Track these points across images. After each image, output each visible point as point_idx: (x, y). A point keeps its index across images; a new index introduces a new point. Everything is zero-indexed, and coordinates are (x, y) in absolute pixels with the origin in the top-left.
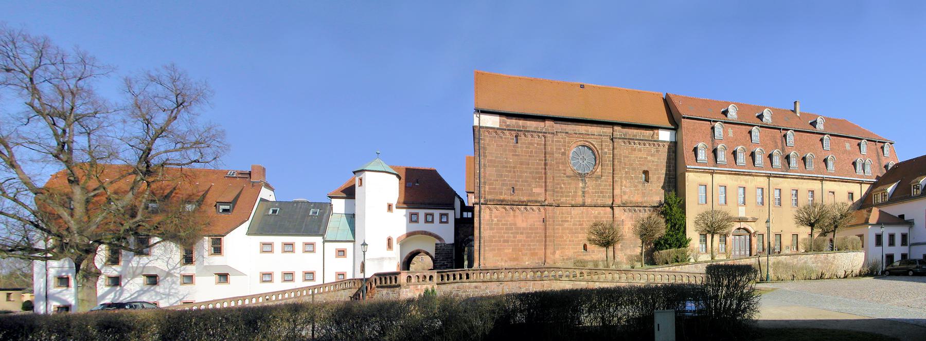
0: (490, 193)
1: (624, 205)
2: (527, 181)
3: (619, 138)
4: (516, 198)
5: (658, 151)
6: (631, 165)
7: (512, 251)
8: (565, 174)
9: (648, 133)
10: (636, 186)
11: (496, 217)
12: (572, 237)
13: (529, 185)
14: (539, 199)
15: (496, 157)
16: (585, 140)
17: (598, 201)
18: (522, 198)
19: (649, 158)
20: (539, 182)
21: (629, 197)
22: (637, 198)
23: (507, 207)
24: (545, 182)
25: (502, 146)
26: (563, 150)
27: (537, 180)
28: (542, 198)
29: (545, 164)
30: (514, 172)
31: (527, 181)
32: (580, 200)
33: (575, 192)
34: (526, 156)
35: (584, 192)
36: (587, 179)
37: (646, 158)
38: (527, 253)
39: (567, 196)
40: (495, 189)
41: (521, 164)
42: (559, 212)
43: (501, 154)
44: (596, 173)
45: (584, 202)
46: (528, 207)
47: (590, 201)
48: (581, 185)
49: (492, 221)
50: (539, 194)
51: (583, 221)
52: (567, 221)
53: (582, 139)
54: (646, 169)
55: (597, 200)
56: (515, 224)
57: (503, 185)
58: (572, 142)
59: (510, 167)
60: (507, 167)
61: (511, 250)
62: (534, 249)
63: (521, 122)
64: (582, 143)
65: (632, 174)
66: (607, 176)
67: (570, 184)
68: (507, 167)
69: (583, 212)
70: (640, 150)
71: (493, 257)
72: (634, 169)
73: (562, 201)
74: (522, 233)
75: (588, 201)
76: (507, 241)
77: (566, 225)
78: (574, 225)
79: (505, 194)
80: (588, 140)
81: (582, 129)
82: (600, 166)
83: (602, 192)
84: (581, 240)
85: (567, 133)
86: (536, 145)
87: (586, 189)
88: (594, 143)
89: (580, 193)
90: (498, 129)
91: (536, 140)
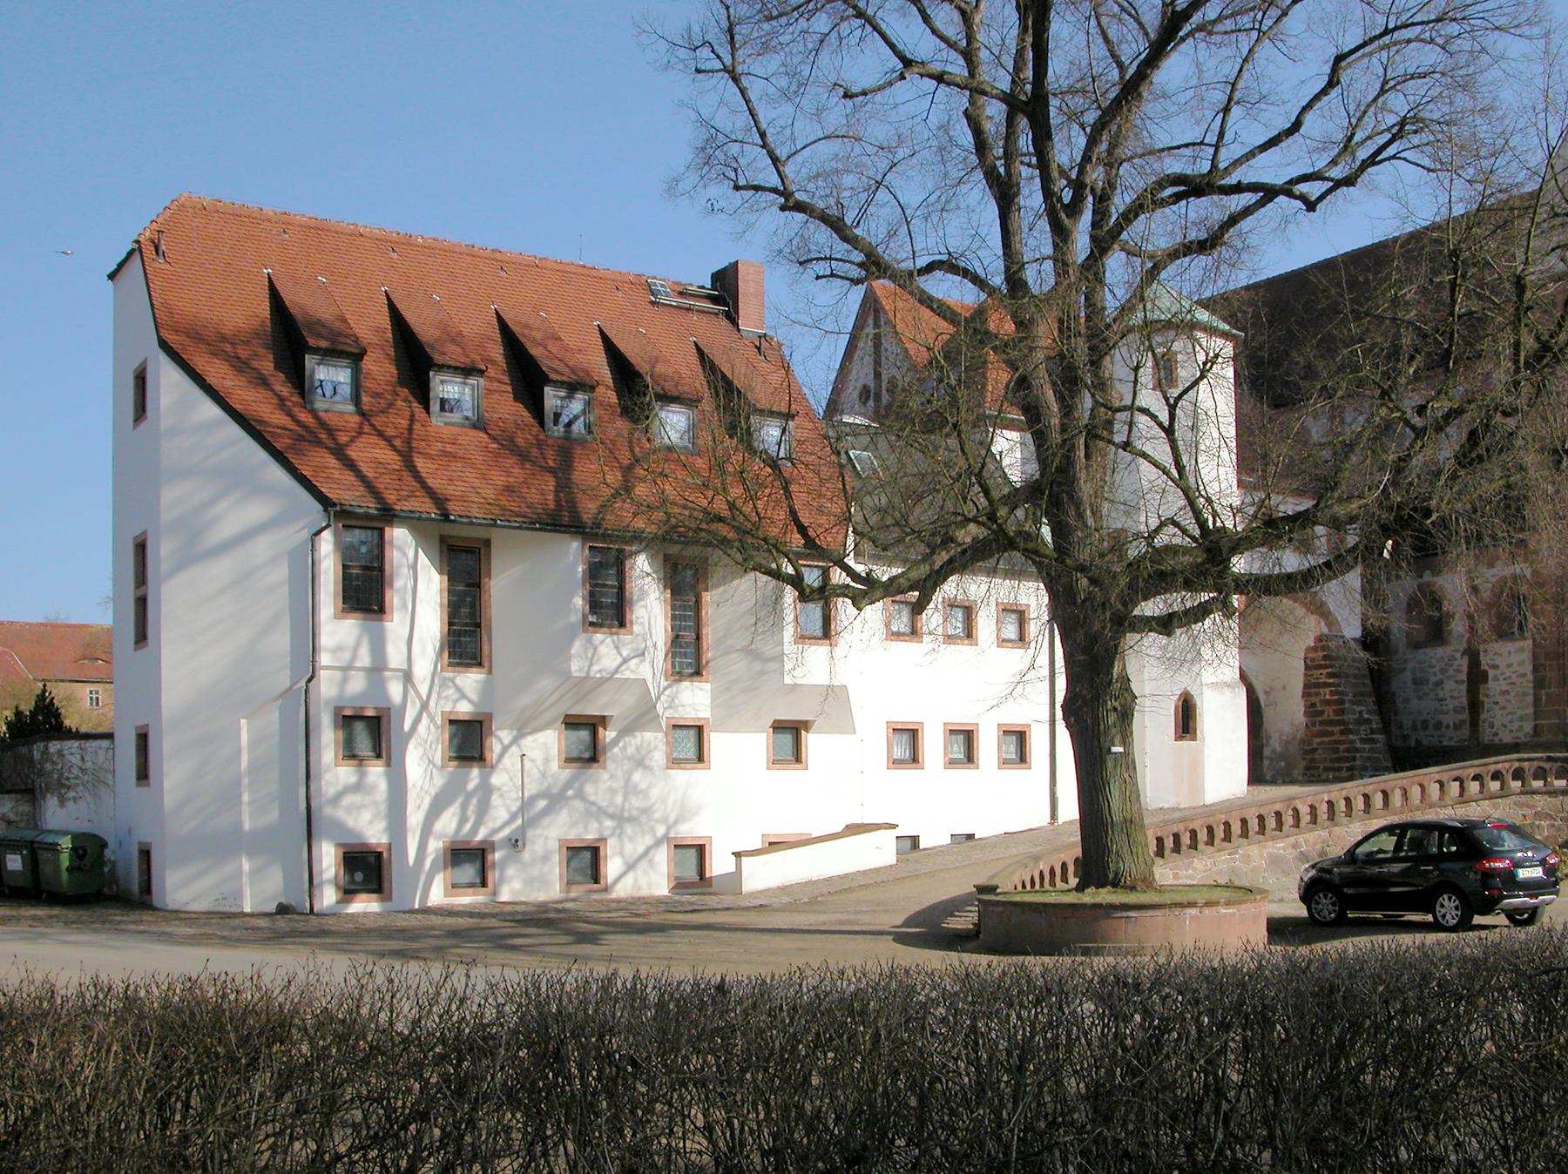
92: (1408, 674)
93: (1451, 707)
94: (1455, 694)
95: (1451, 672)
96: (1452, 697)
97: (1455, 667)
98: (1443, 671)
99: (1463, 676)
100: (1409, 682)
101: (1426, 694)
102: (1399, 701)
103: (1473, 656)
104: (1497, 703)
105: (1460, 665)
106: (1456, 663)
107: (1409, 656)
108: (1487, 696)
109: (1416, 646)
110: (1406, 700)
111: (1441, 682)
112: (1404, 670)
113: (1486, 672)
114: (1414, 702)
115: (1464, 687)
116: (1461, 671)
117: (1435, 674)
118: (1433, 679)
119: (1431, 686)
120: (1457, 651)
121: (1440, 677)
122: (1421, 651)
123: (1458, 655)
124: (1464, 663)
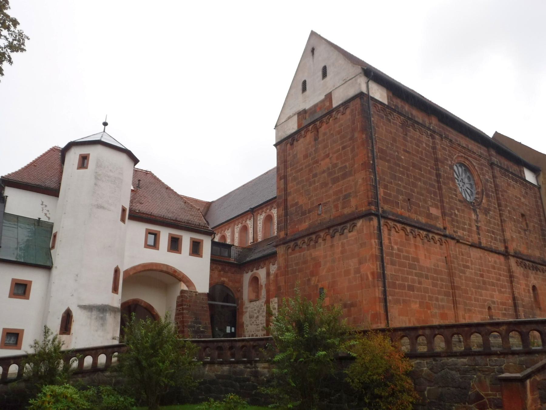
0: (386, 201)
1: (517, 255)
2: (422, 195)
3: (498, 166)
4: (414, 217)
5: (526, 193)
6: (511, 203)
7: (420, 306)
8: (456, 195)
9: (514, 168)
10: (520, 233)
11: (396, 244)
12: (476, 293)
13: (425, 201)
14: (438, 225)
15: (387, 147)
16: (466, 156)
17: (492, 244)
18: (420, 218)
19: (523, 200)
20: (434, 199)
21: (517, 245)
22: (523, 249)
23: (408, 229)
24: (442, 201)
25: (391, 133)
26: (450, 163)
27: (432, 196)
28: (440, 225)
29: (438, 175)
30: (408, 176)
31: (422, 195)
32: (474, 238)
33: (470, 225)
34: (417, 157)
35: (478, 228)
36: (478, 210)
37: (520, 199)
38: (436, 313)
39: (464, 229)
40: (390, 195)
41: (414, 166)
42: (459, 251)
43: (392, 145)
44: (482, 205)
45: (480, 243)
46: (431, 235)
47: (484, 242)
48: (474, 217)
49: (392, 249)
50: (437, 218)
51: (483, 271)
52: (468, 267)
53: (463, 155)
54: (523, 212)
55: (491, 242)
56: (417, 260)
57: (399, 192)
58: (455, 155)
59: (403, 167)
60: (399, 166)
61: (418, 305)
62: (443, 307)
63: (407, 108)
64: (462, 160)
65: (514, 216)
66: (494, 212)
67: (463, 211)
68: (399, 166)
69: (481, 256)
70: (514, 187)
71: (399, 315)
72: (514, 210)
73: (459, 234)
74: (427, 277)
75: (484, 243)
76: (411, 288)
77: (468, 271)
78: (476, 274)
79: (402, 208)
80: (469, 158)
81: (464, 141)
82: (484, 196)
83: (493, 233)
84: (485, 301)
85: (451, 141)
86: (424, 145)
87: (479, 225)
88: (475, 164)
89: (474, 228)
90: (388, 107)
91: (424, 138)
93: (261, 328)
94: (262, 322)
95: (261, 312)
96: (261, 324)
98: (259, 312)
99: (264, 314)
101: (253, 322)
102: (245, 326)
103: (268, 302)
105: (263, 309)
106: (262, 308)
107: (248, 306)
109: (251, 301)
110: (247, 326)
111: (257, 317)
112: (246, 312)
114: (250, 326)
115: (265, 319)
117: (256, 314)
118: (255, 315)
119: (254, 319)
120: (263, 302)
121: (258, 314)
123: (263, 304)
124: (265, 307)
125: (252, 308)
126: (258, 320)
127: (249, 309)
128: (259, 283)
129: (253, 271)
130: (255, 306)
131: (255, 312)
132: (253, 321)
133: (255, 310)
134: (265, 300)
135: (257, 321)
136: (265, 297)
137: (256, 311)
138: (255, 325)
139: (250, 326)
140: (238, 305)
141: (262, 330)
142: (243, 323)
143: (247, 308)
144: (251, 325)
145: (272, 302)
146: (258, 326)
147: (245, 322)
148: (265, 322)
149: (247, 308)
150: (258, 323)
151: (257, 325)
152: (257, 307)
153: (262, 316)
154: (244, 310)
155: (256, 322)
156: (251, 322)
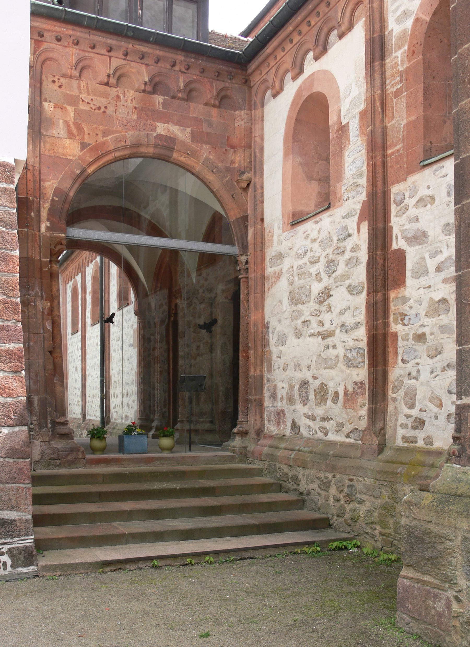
92: (283, 284)
93: (340, 351)
94: (349, 319)
95: (341, 268)
97: (347, 255)
100: (286, 301)
101: (306, 323)
104: (420, 338)
105: (354, 249)
106: (349, 244)
107: (282, 249)
108: (402, 317)
110: (282, 341)
112: (278, 276)
113: (401, 254)
114: (292, 340)
116: (358, 263)
117: (318, 277)
118: (317, 288)
119: (312, 306)
121: (326, 281)
122: (301, 228)
123: (352, 223)
125: (299, 256)
126: (329, 309)
127: (286, 264)
128: (333, 119)
129: (301, 71)
130: (314, 240)
131: (314, 269)
132: (306, 316)
133: (314, 262)
134: (363, 197)
135: (326, 317)
136: (364, 181)
137: (321, 266)
138: (313, 335)
139: (292, 340)
140: (244, 248)
141: (349, 363)
142: (266, 326)
143: (280, 257)
144: (298, 335)
145: (398, 203)
146: (330, 341)
147: (273, 323)
148: (361, 316)
149: (280, 257)
150: (327, 326)
151: (326, 335)
152: (324, 244)
153: (350, 290)
154: (270, 270)
155: (321, 323)
156: (299, 322)
